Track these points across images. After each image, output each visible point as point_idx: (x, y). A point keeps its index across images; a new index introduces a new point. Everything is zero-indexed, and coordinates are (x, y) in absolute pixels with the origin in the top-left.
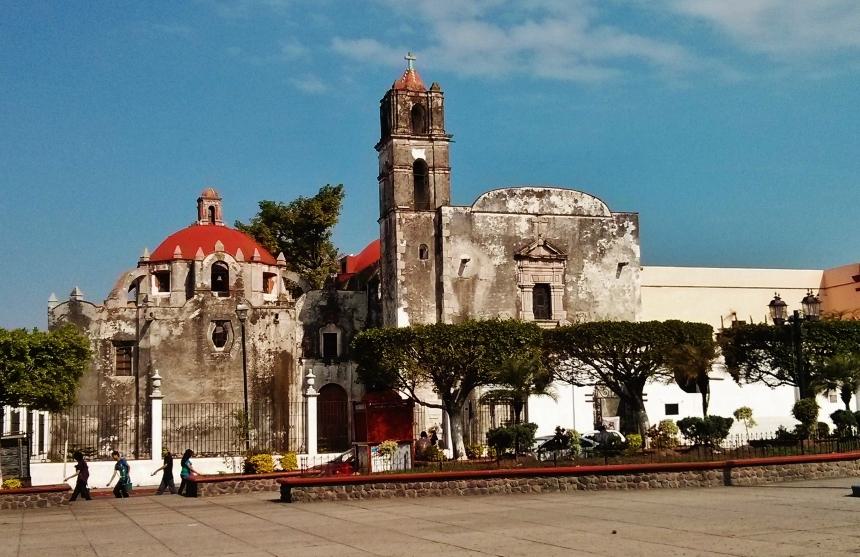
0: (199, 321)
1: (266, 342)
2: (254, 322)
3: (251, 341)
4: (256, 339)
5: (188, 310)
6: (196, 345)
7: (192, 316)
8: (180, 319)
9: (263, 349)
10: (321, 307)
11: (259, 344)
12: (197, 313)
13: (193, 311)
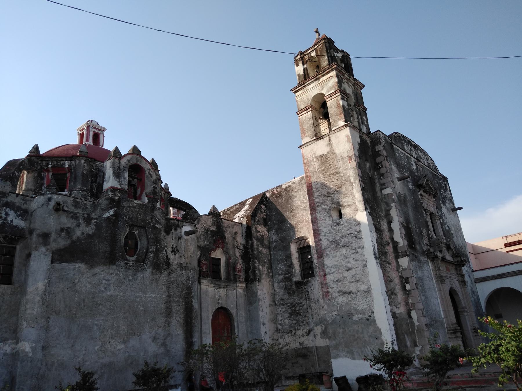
0: (114, 221)
1: (178, 255)
2: (168, 233)
3: (164, 252)
4: (169, 251)
5: (103, 206)
6: (108, 249)
7: (107, 215)
8: (93, 215)
9: (175, 262)
10: (212, 231)
11: (171, 257)
12: (111, 213)
13: (107, 210)
